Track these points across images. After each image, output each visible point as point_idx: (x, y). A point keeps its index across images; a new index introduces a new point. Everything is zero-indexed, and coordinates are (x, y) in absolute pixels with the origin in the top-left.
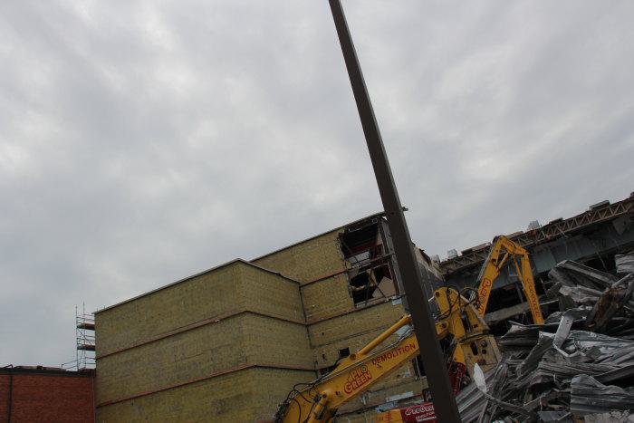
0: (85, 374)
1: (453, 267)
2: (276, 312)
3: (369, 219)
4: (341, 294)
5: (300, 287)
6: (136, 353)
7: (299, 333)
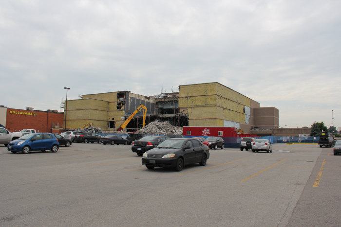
0: (63, 113)
1: (158, 100)
2: (99, 108)
3: (124, 92)
4: (114, 106)
5: (108, 102)
6: (71, 111)
7: (105, 113)
